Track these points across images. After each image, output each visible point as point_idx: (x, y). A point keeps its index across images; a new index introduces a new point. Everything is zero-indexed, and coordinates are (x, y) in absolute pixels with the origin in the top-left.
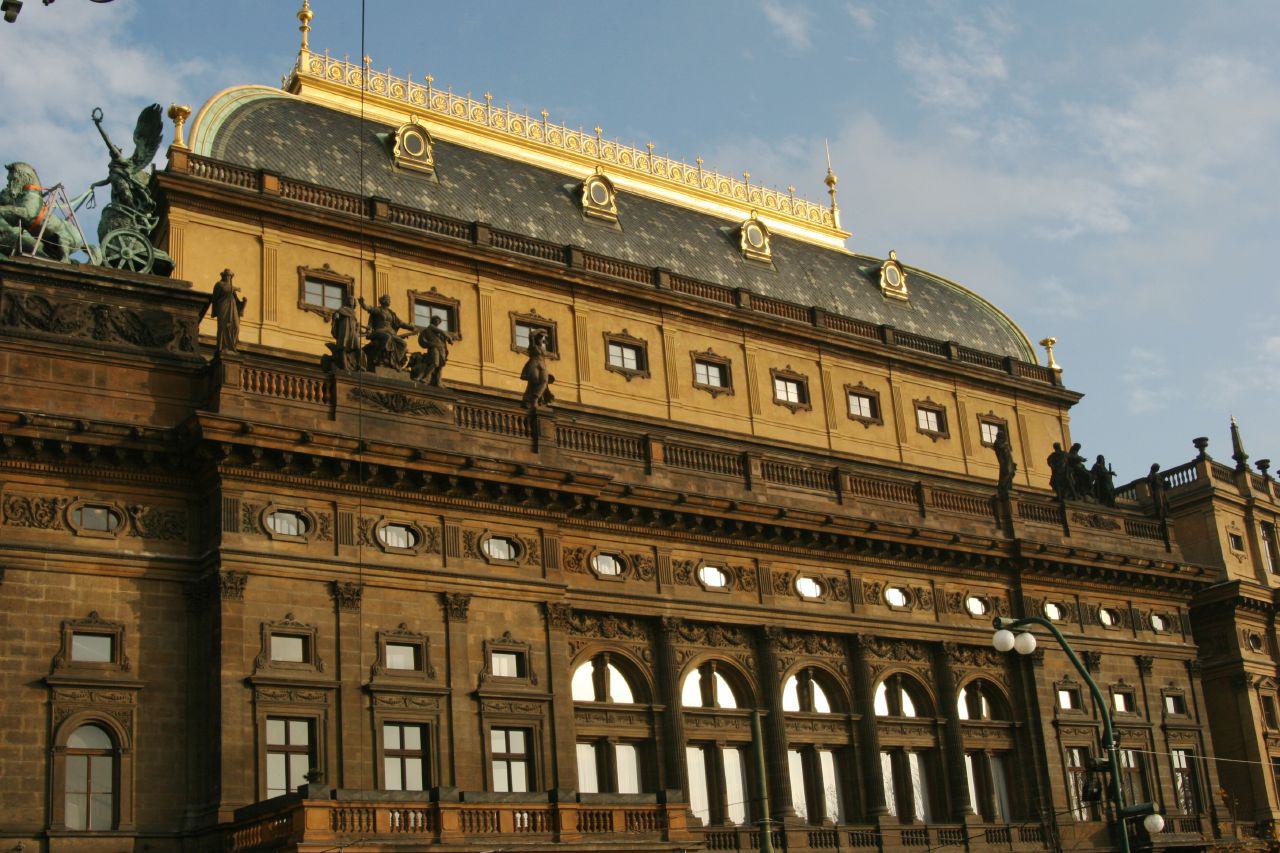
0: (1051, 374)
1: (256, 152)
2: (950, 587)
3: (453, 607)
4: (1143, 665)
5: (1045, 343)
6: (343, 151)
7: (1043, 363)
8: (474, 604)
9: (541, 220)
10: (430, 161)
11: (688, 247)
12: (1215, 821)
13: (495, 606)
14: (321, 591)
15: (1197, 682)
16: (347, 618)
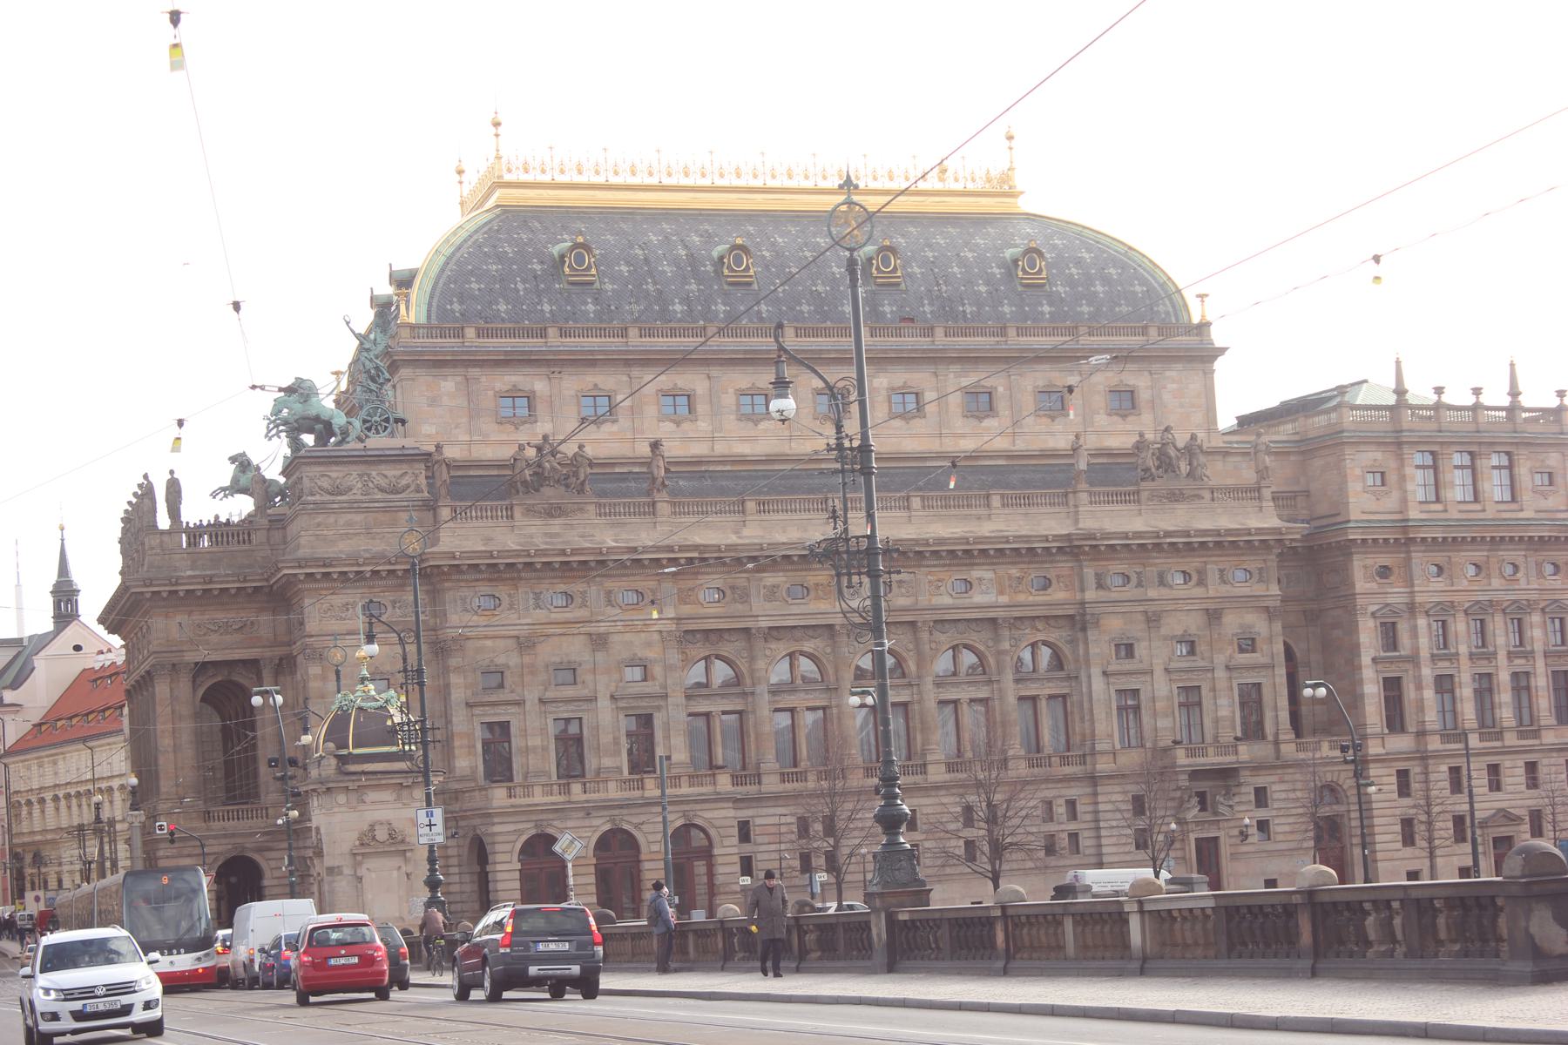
0: (1204, 327)
1: (461, 303)
2: (1014, 571)
3: (599, 642)
4: (1213, 616)
5: (1202, 296)
6: (524, 281)
7: (1196, 320)
8: (615, 638)
9: (686, 300)
10: (593, 271)
11: (820, 288)
12: (1277, 743)
13: (628, 637)
14: (511, 643)
15: (1278, 626)
16: (527, 659)
